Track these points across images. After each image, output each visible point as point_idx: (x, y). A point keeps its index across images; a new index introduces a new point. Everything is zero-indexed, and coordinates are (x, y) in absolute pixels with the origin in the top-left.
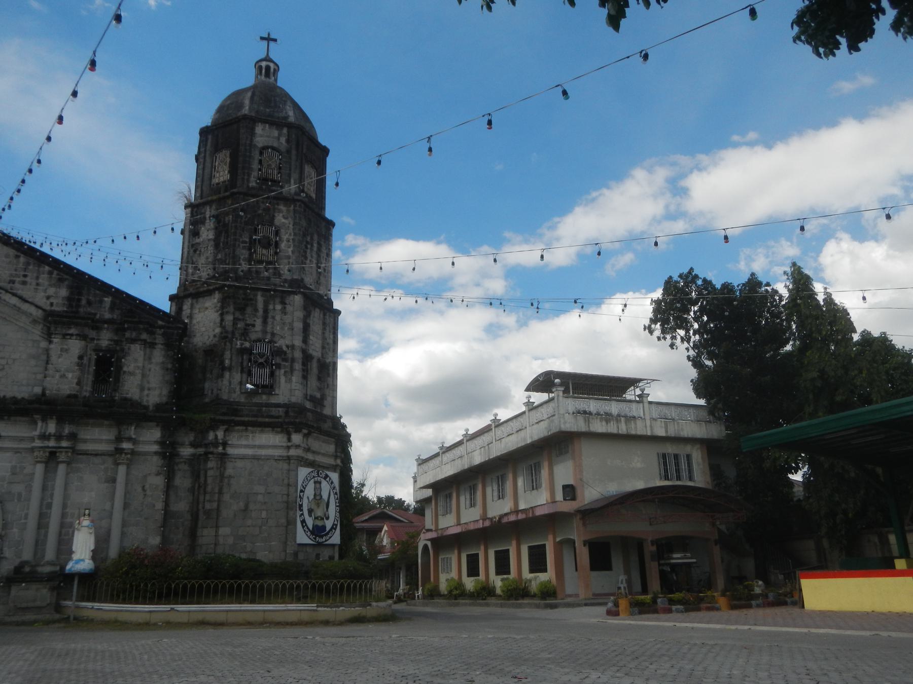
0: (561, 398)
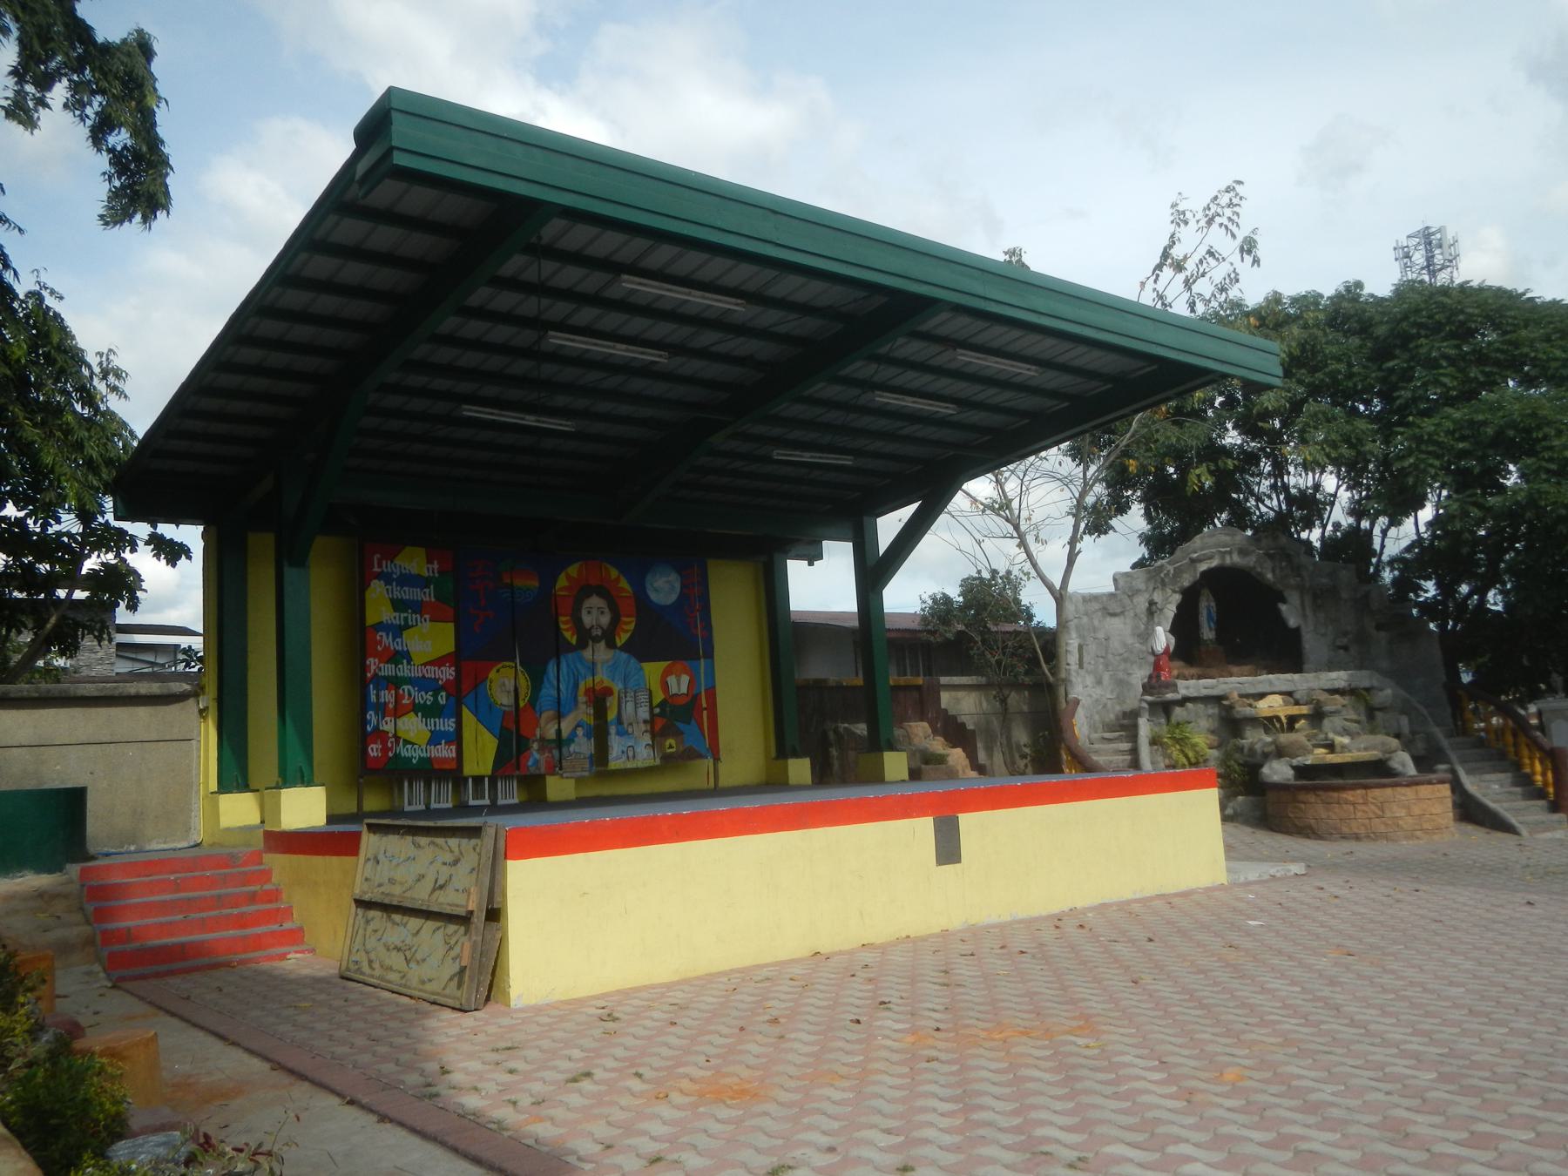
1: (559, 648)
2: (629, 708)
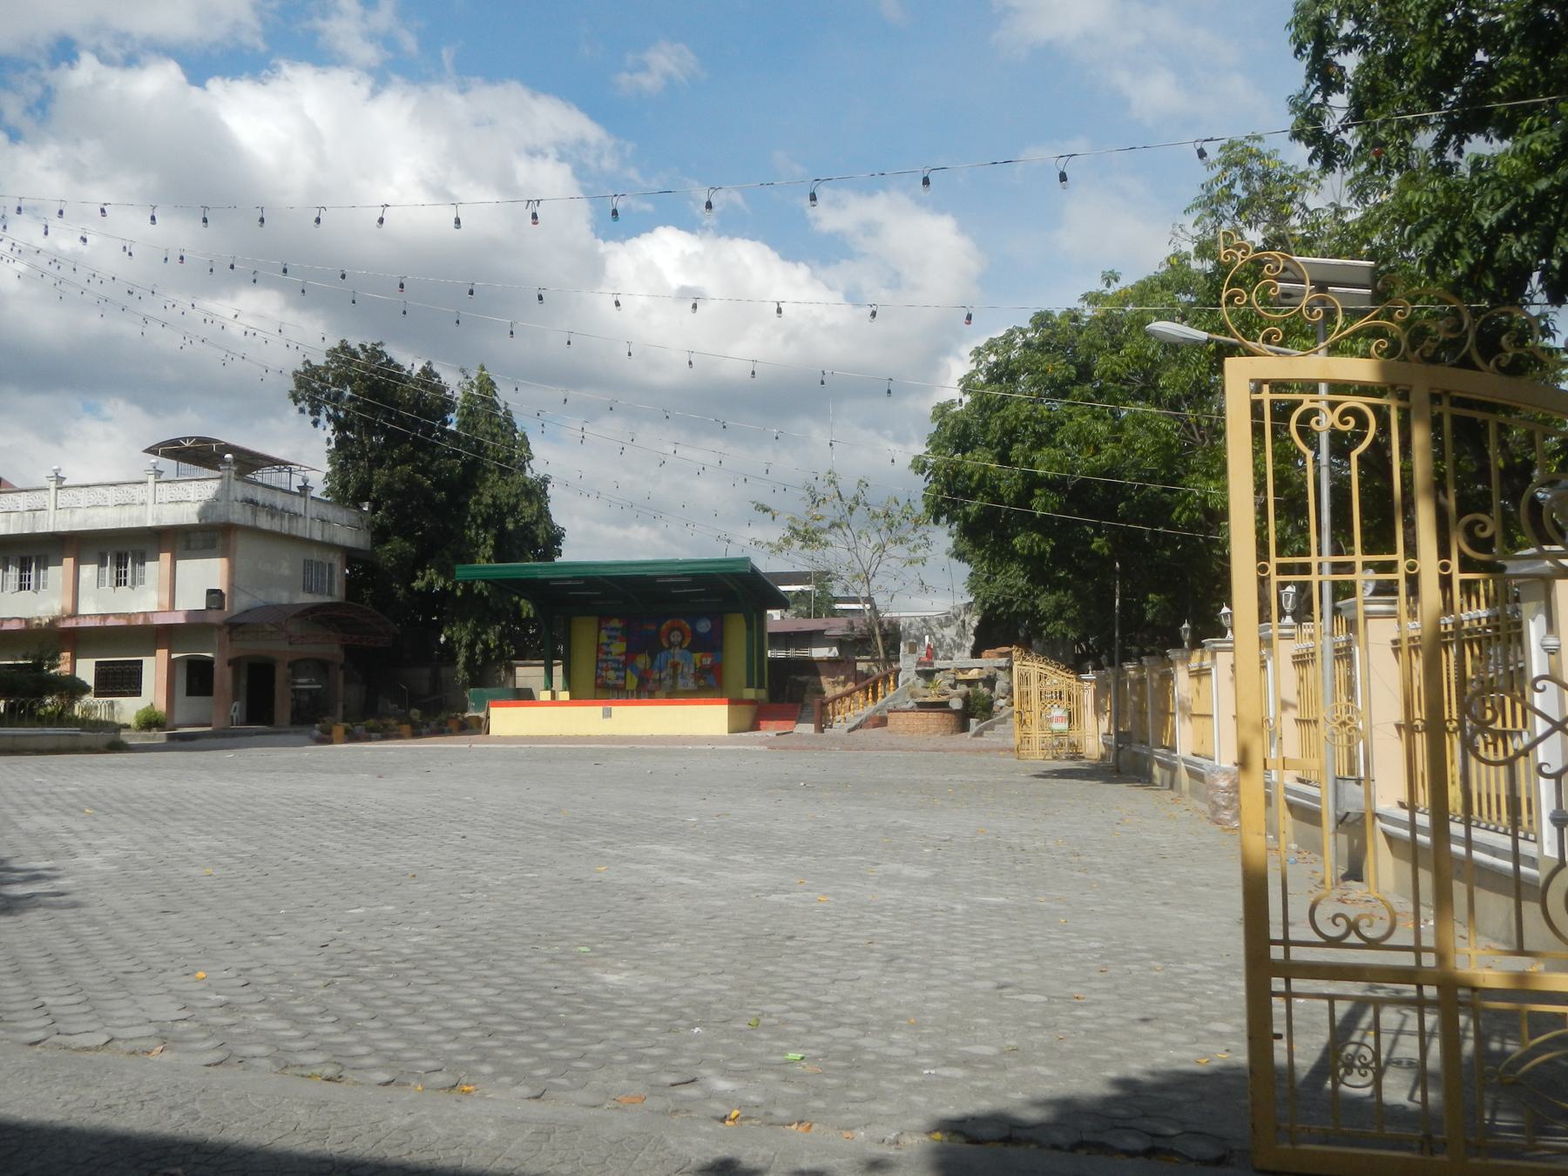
0: (232, 480)
1: (662, 649)
2: (686, 669)
